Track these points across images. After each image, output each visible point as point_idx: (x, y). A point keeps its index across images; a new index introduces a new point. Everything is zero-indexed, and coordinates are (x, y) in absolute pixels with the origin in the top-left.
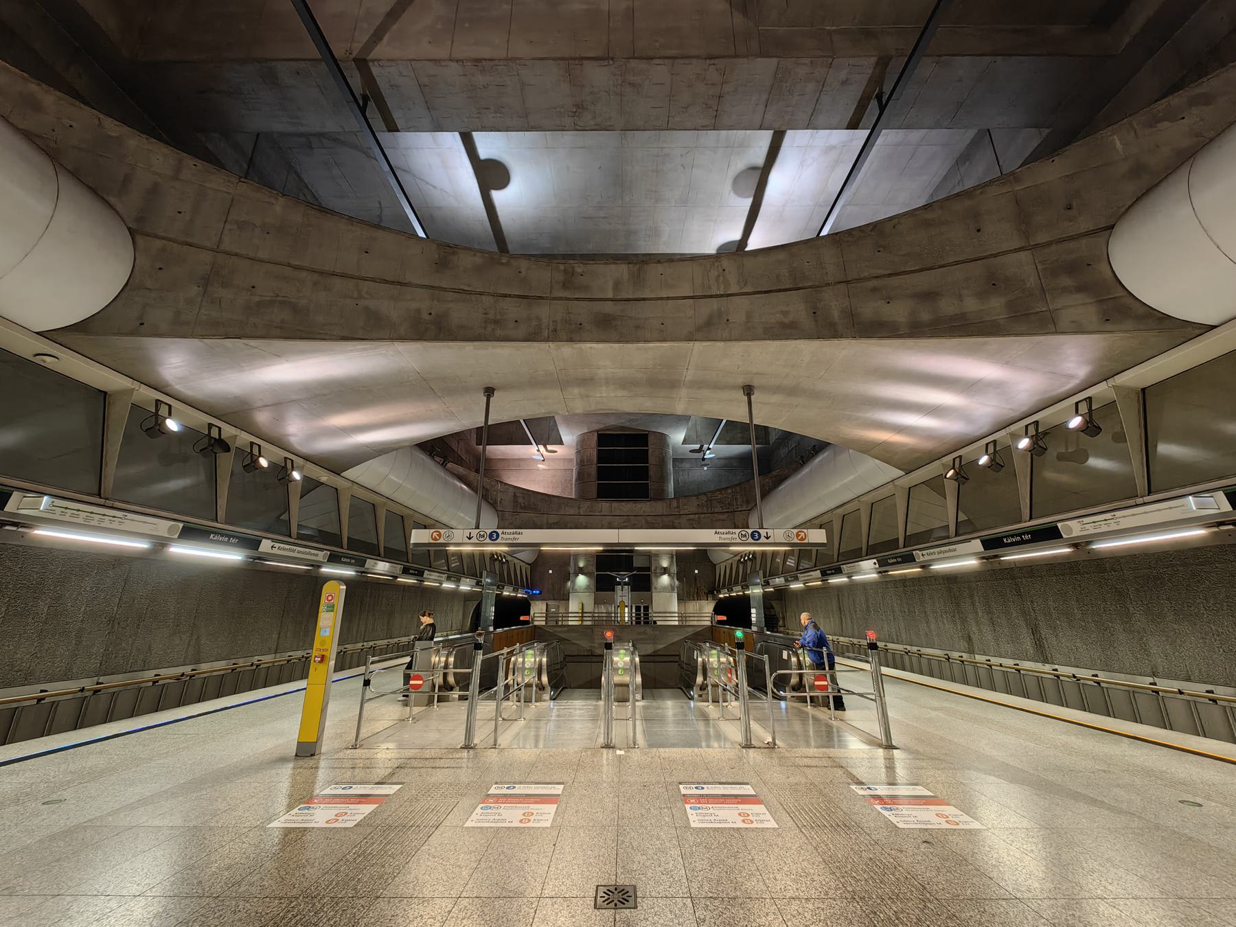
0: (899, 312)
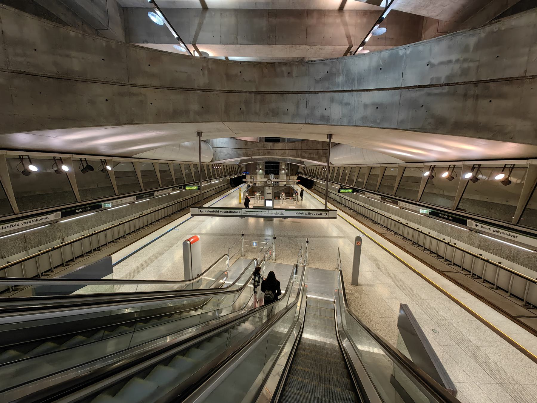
0: (306, 155)
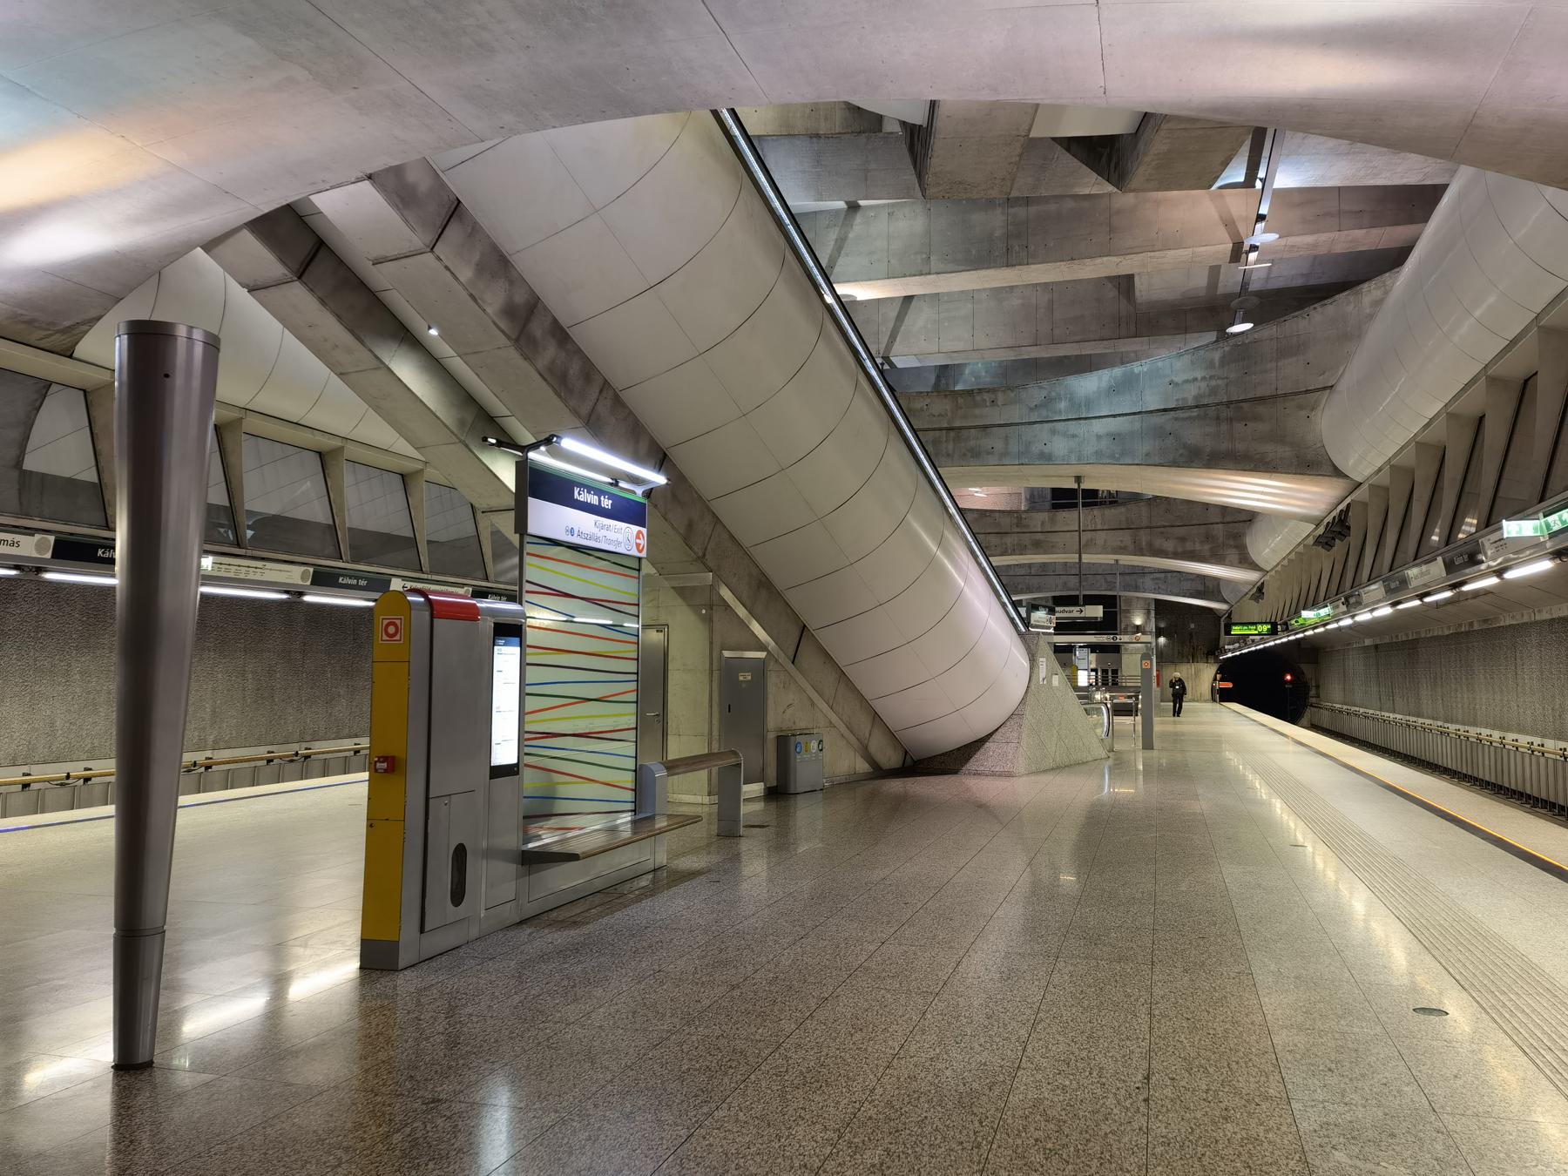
0: (1169, 545)
